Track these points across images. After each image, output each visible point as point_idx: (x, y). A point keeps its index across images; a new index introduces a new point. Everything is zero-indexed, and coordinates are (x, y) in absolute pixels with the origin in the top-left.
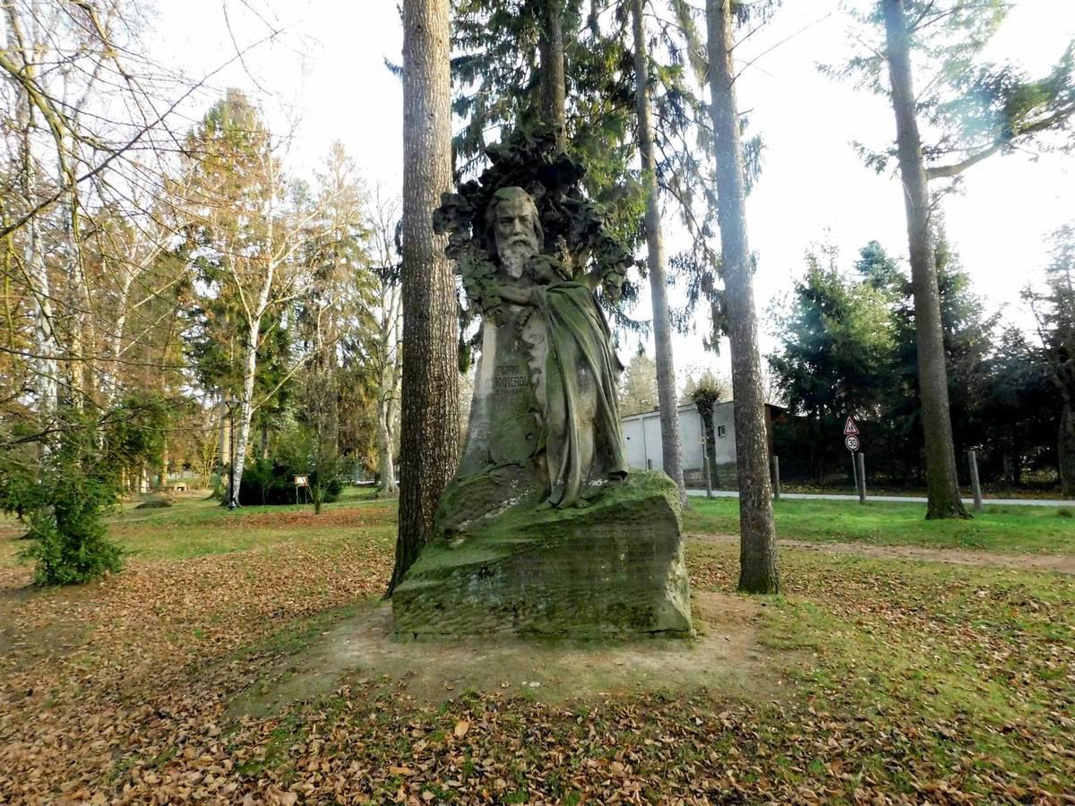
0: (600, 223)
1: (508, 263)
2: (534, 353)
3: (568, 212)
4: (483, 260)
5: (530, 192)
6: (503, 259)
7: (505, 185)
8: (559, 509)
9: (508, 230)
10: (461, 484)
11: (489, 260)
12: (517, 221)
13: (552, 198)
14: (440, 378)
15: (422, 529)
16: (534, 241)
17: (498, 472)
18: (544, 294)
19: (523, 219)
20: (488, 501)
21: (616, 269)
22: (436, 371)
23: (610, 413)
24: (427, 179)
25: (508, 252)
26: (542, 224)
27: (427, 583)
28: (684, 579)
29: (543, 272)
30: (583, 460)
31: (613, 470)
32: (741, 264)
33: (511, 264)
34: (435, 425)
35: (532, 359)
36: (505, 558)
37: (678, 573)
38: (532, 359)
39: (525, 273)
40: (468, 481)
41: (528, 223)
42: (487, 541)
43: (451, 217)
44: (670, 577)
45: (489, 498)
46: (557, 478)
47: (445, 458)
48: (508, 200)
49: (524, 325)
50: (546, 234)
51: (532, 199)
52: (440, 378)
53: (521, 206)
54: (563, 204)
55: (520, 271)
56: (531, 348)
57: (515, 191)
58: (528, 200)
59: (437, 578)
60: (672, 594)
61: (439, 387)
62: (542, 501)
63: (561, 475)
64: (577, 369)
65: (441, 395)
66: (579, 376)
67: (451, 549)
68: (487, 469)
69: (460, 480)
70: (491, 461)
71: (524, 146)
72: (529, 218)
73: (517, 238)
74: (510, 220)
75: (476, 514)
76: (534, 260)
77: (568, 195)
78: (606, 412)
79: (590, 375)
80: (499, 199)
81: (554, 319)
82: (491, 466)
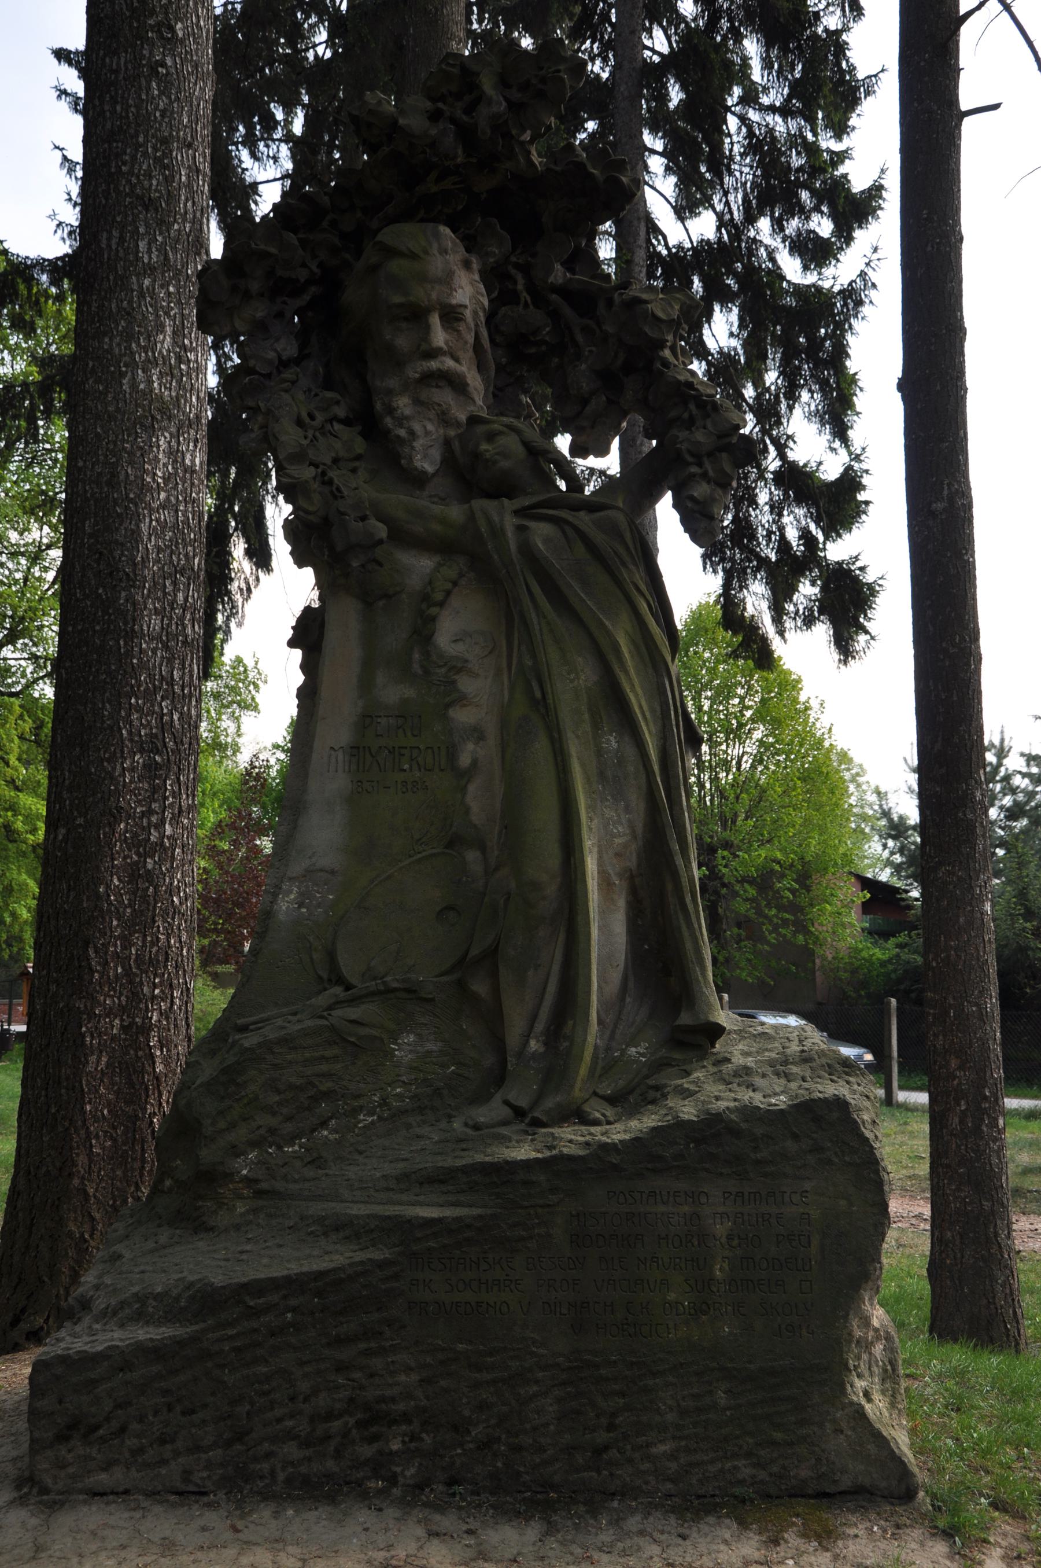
0: (662, 344)
1: (402, 433)
2: (466, 685)
3: (567, 311)
4: (331, 421)
5: (470, 243)
6: (388, 421)
7: (406, 215)
8: (537, 1123)
9: (403, 342)
10: (249, 1041)
11: (347, 422)
12: (435, 320)
13: (525, 269)
14: (152, 745)
15: (82, 1160)
16: (475, 381)
17: (353, 1013)
18: (510, 522)
19: (451, 316)
20: (327, 1095)
21: (708, 466)
22: (144, 726)
23: (679, 861)
24: (149, 204)
25: (403, 404)
26: (492, 341)
27: (143, 1334)
28: (888, 1338)
29: (505, 464)
30: (603, 979)
31: (685, 1019)
32: (951, 500)
33: (412, 433)
34: (135, 874)
35: (462, 700)
36: (382, 1265)
37: (875, 1323)
38: (462, 700)
39: (449, 461)
40: (270, 1033)
41: (462, 327)
42: (317, 1209)
43: (255, 286)
44: (858, 1333)
45: (326, 1085)
46: (527, 1037)
47: (153, 962)
48: (413, 256)
49: (441, 604)
50: (499, 368)
51: (475, 266)
52: (152, 745)
53: (447, 280)
54: (555, 289)
55: (436, 454)
56: (459, 671)
57: (437, 235)
58: (467, 265)
59: (170, 1316)
60: (860, 1384)
61: (151, 767)
62: (480, 1098)
63: (540, 1027)
64: (596, 725)
65: (156, 791)
66: (599, 753)
67: (212, 1229)
68: (321, 1000)
69: (244, 1029)
70: (339, 980)
71: (469, 110)
72: (468, 313)
73: (434, 365)
74: (417, 315)
75: (289, 1127)
76: (480, 429)
77: (569, 265)
78: (669, 856)
79: (630, 751)
80: (391, 252)
81: (537, 590)
82: (338, 990)
